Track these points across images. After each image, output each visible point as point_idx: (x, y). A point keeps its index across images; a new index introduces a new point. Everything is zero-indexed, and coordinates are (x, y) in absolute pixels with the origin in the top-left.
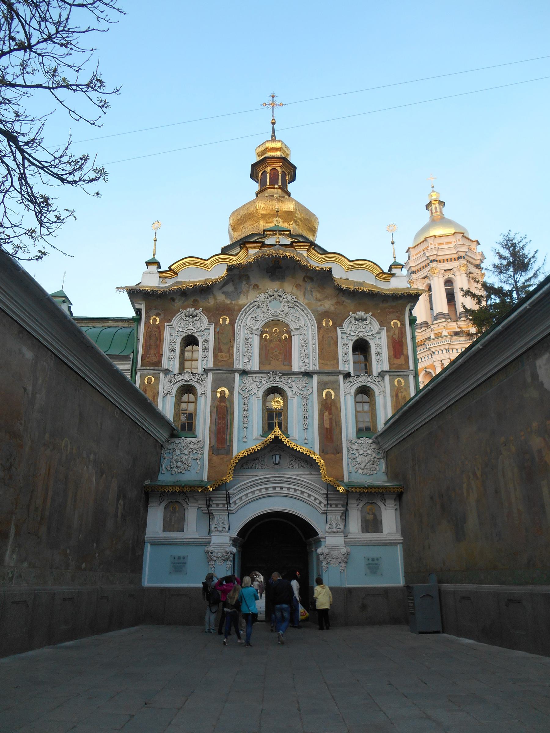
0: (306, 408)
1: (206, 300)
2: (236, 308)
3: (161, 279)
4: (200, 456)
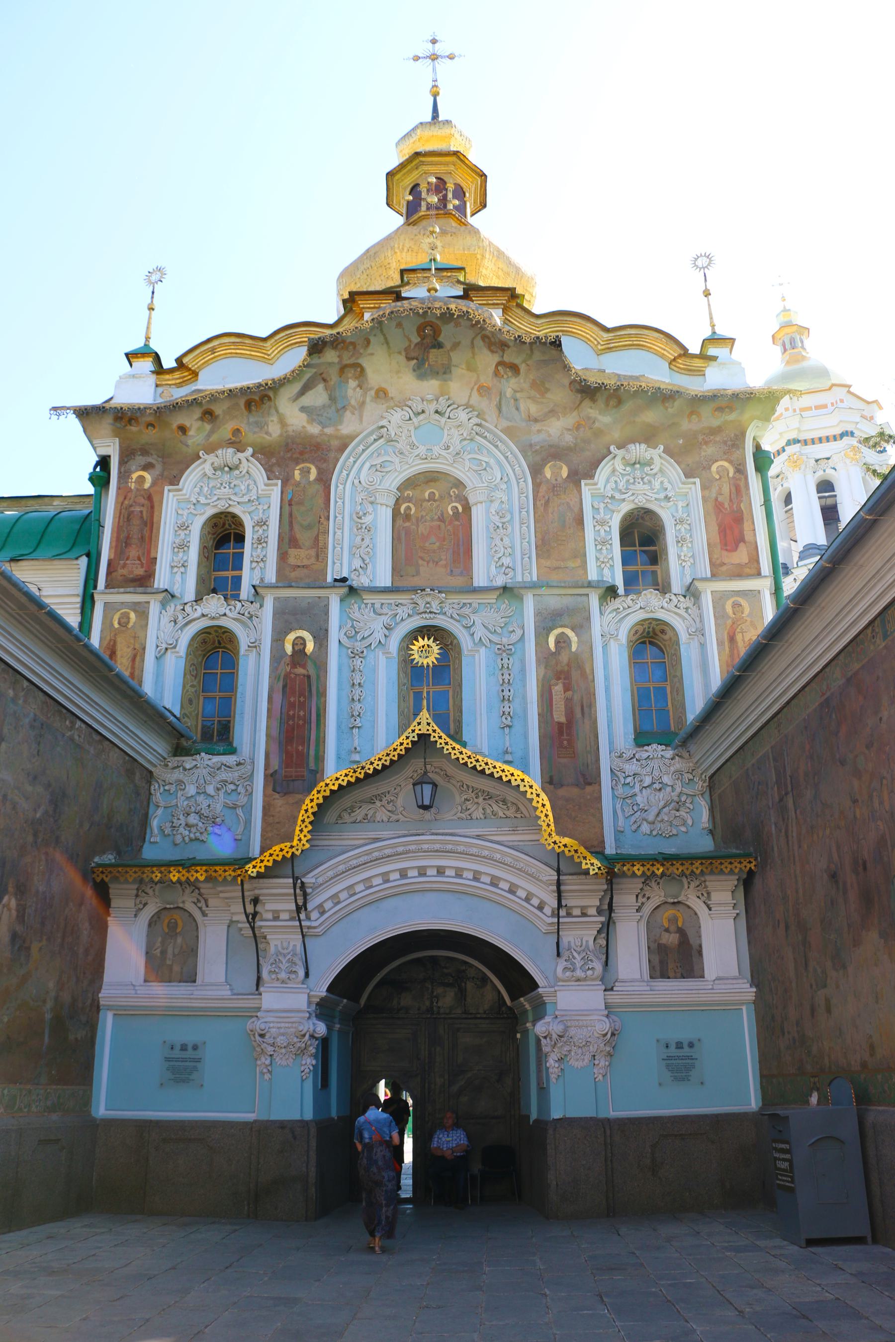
0: (506, 677)
1: (262, 428)
2: (335, 443)
3: (160, 390)
4: (243, 800)
